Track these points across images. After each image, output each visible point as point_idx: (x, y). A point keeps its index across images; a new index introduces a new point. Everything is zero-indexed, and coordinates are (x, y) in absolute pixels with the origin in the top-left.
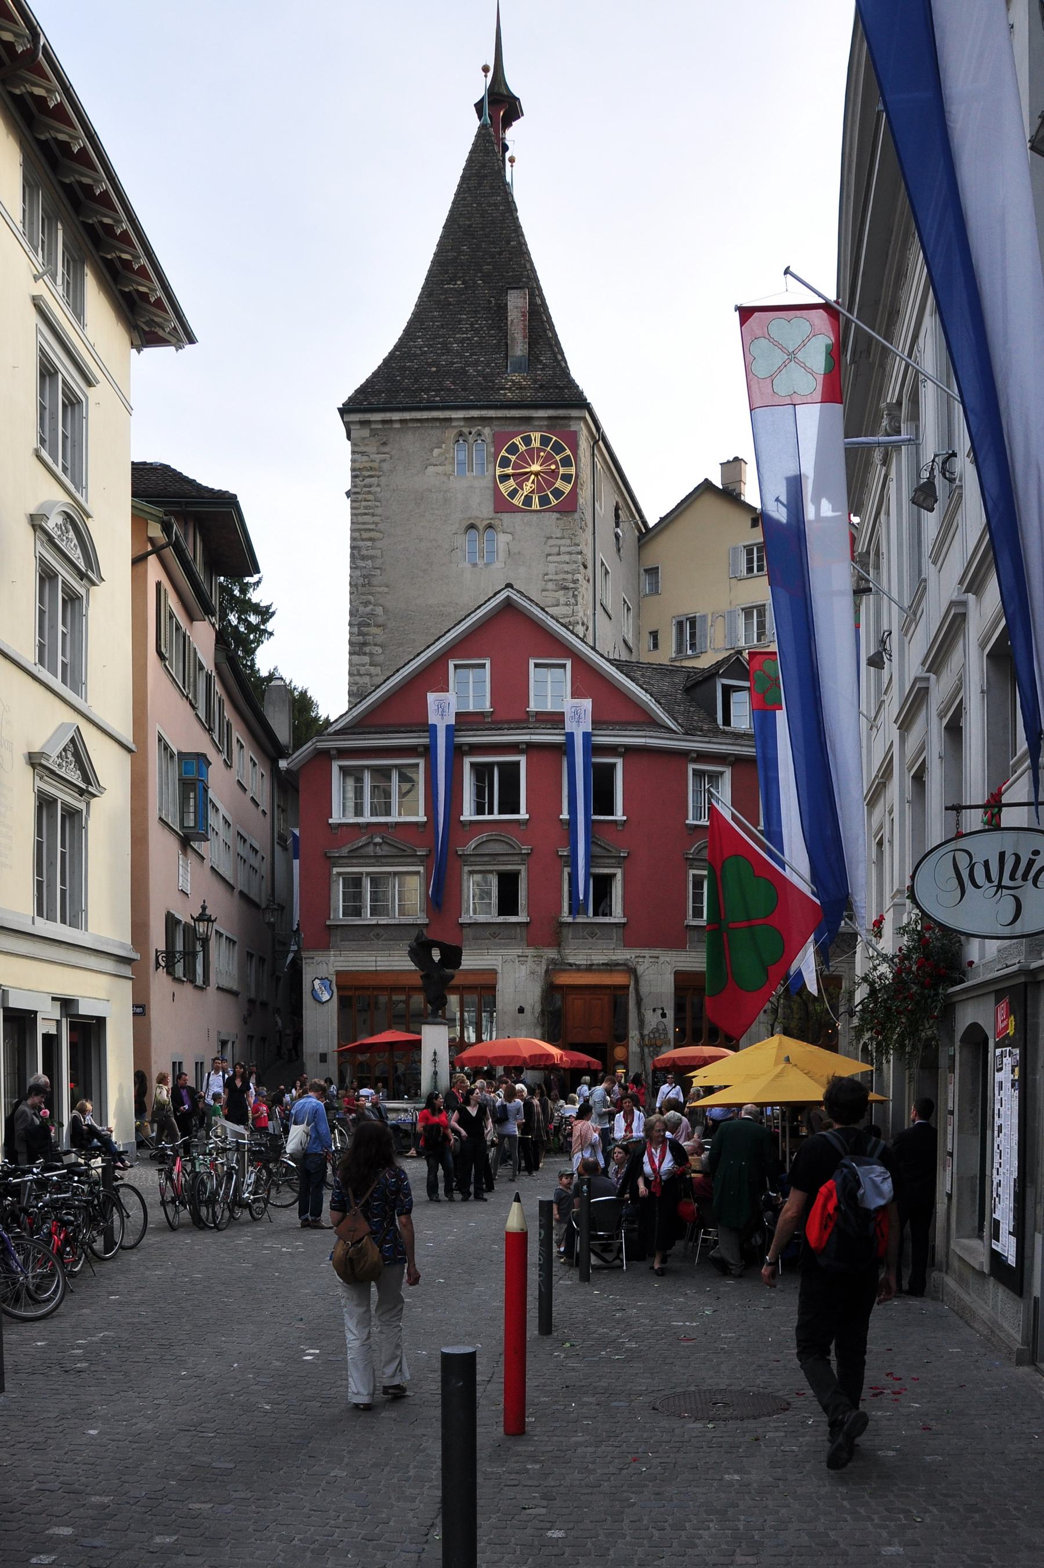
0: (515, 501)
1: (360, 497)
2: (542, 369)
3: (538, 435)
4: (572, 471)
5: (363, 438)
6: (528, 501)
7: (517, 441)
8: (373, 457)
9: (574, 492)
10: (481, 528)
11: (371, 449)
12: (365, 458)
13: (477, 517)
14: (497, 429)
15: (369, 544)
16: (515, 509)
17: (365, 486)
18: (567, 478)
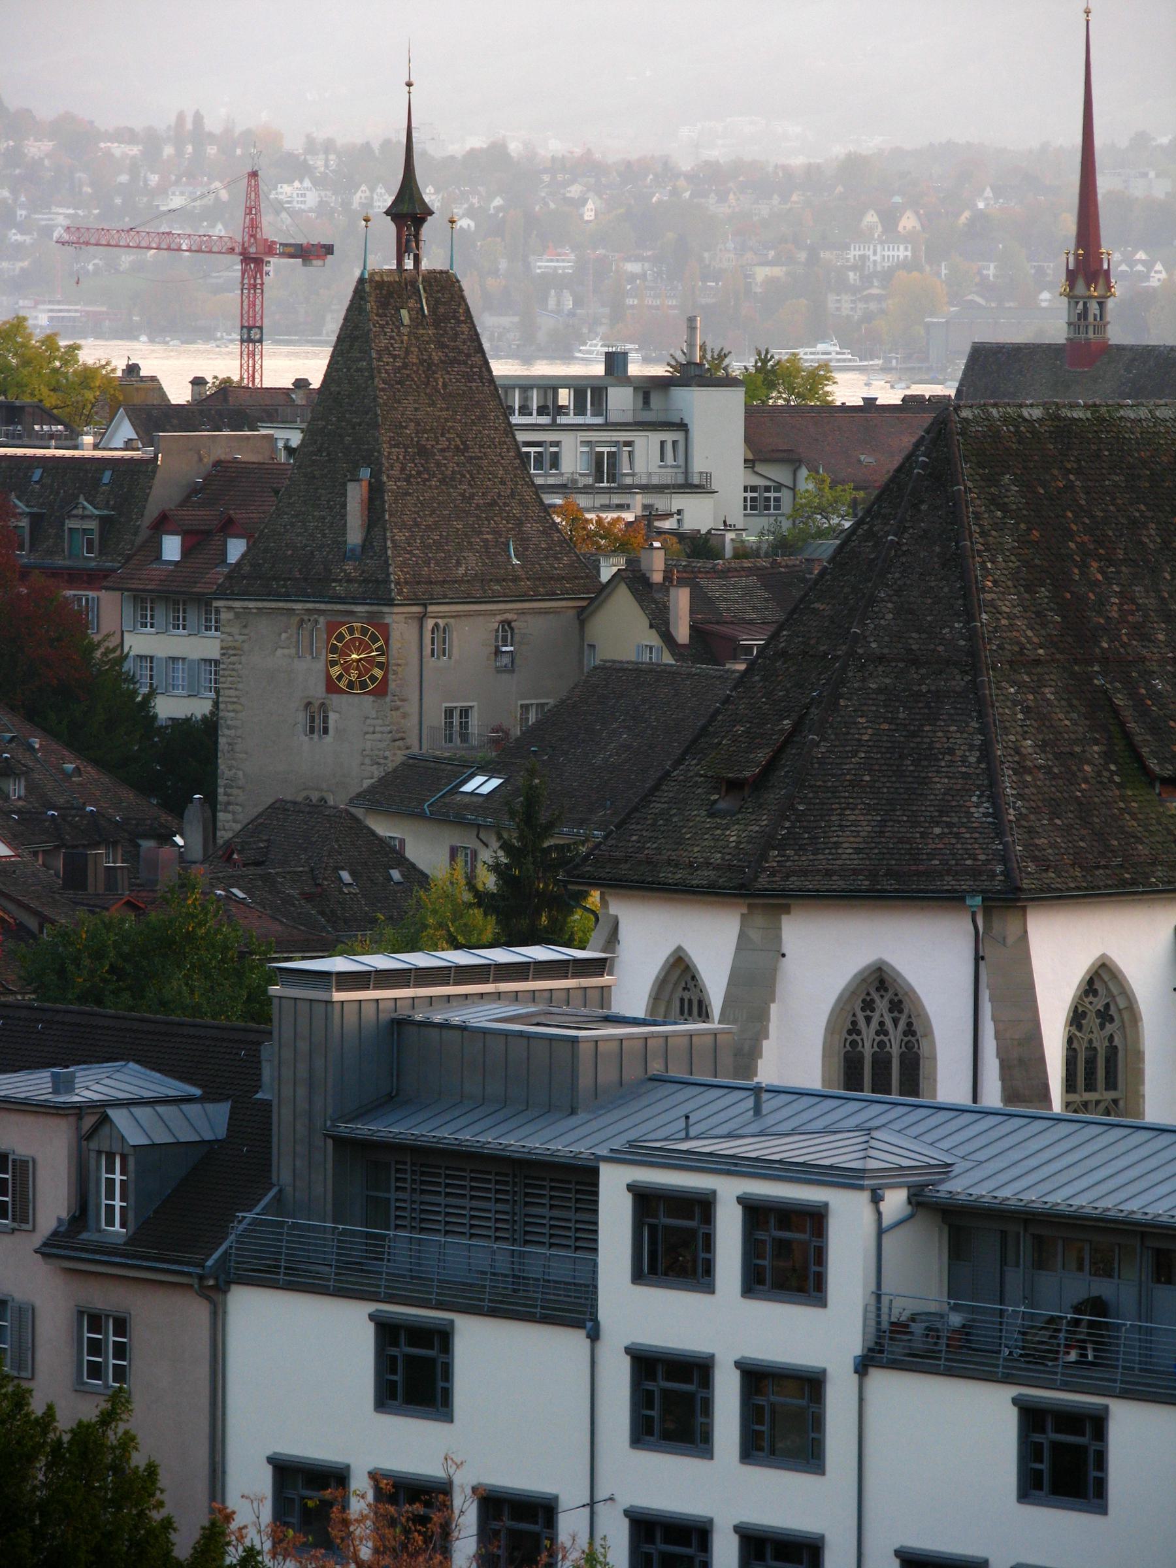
7: (343, 629)
8: (237, 637)
9: (385, 677)
12: (230, 638)
14: (329, 618)
15: (232, 714)
16: (340, 691)
18: (380, 666)
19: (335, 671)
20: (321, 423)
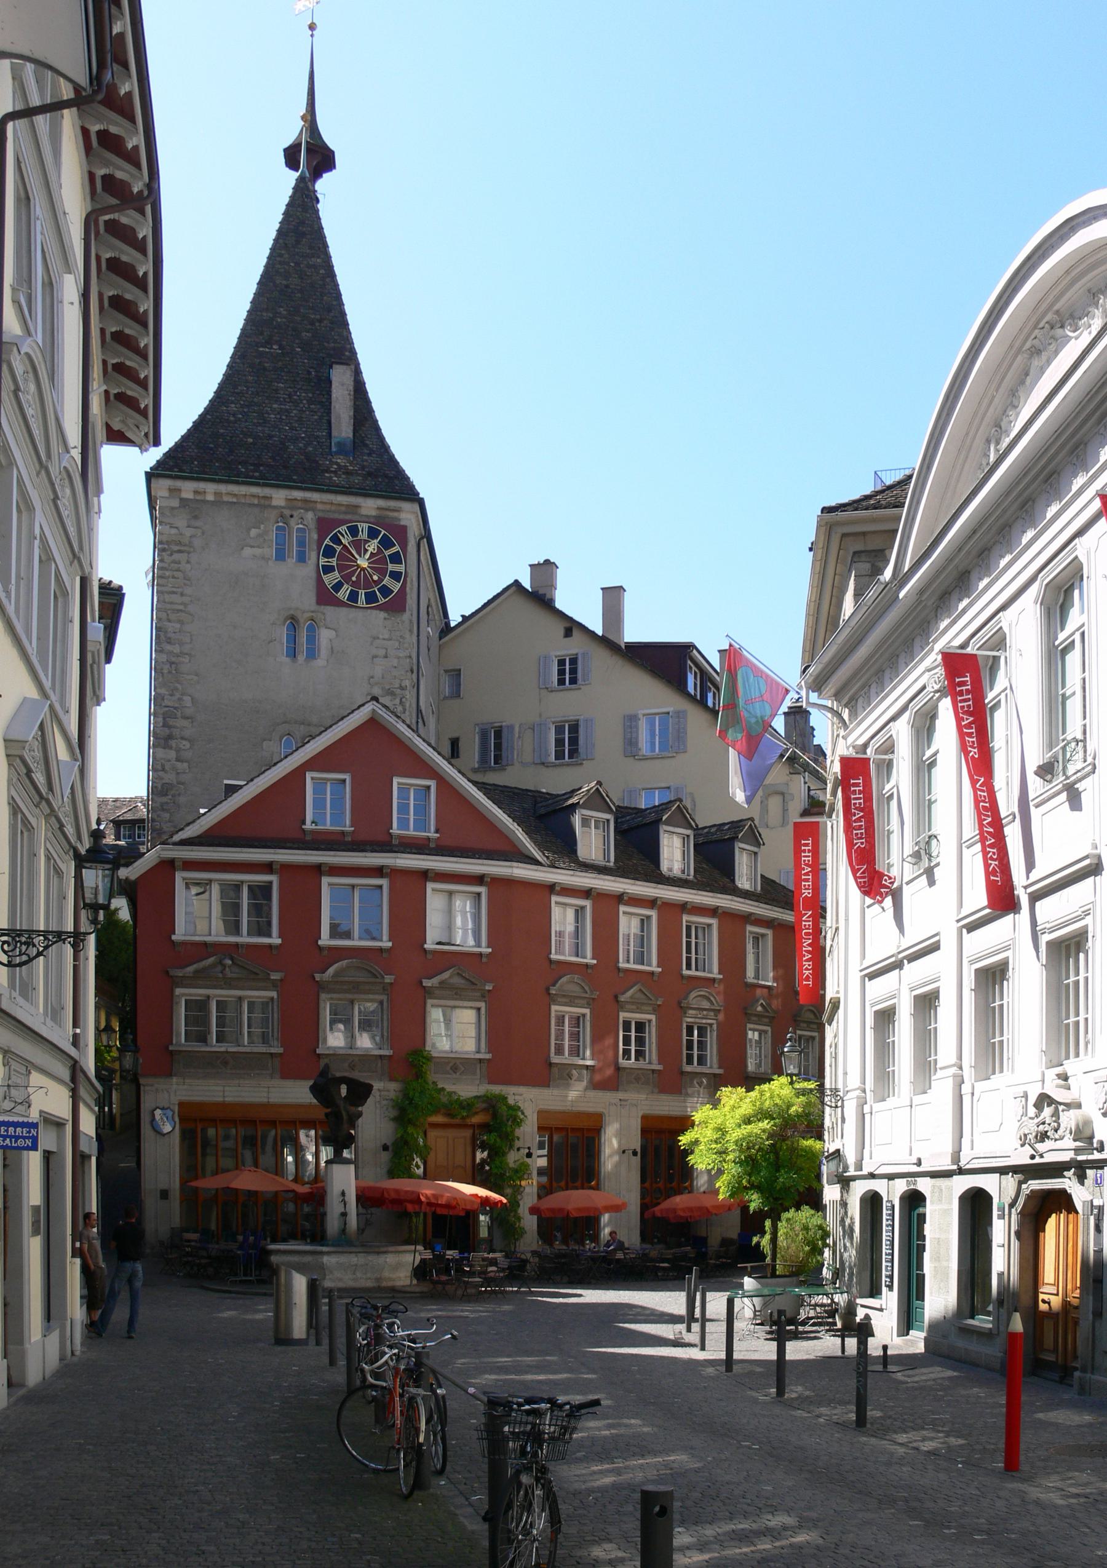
0: (340, 595)
1: (167, 573)
2: (369, 455)
3: (366, 526)
4: (401, 568)
5: (173, 508)
6: (353, 597)
7: (343, 529)
9: (403, 589)
10: (302, 621)
11: (181, 522)
12: (174, 531)
13: (297, 609)
14: (320, 514)
16: (339, 603)
17: (174, 562)
18: (396, 576)
19: (330, 579)
20: (266, 315)
